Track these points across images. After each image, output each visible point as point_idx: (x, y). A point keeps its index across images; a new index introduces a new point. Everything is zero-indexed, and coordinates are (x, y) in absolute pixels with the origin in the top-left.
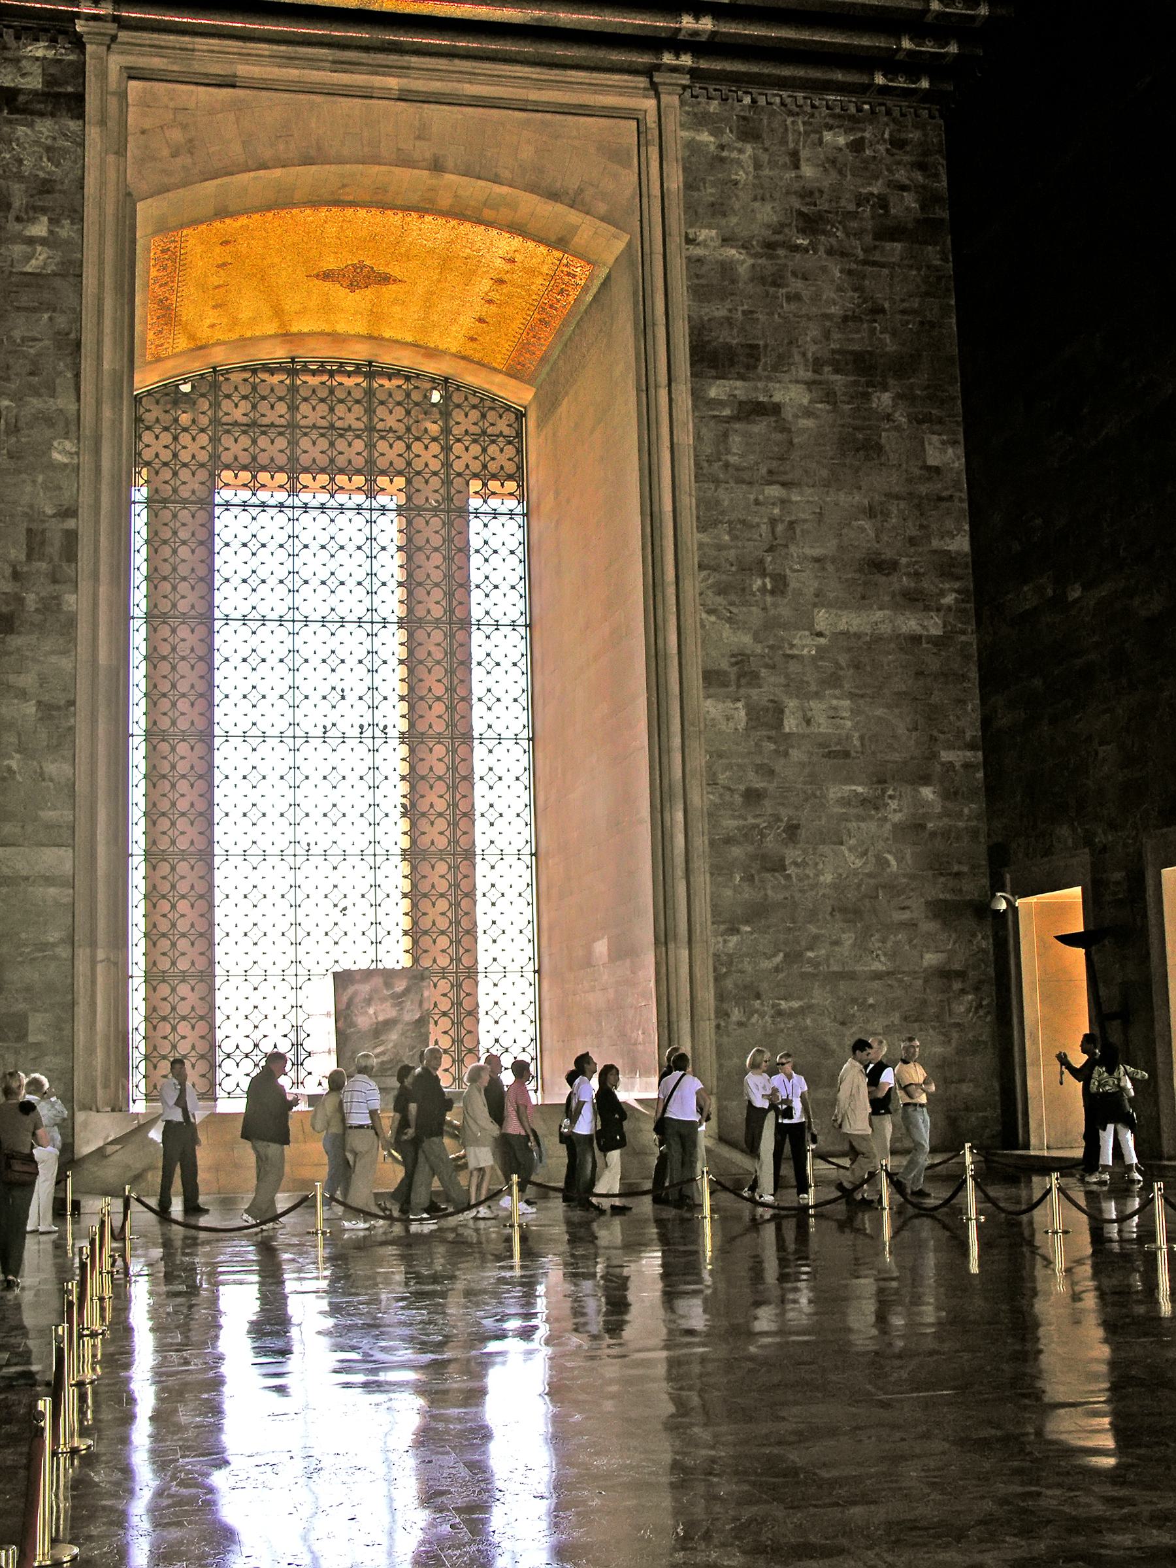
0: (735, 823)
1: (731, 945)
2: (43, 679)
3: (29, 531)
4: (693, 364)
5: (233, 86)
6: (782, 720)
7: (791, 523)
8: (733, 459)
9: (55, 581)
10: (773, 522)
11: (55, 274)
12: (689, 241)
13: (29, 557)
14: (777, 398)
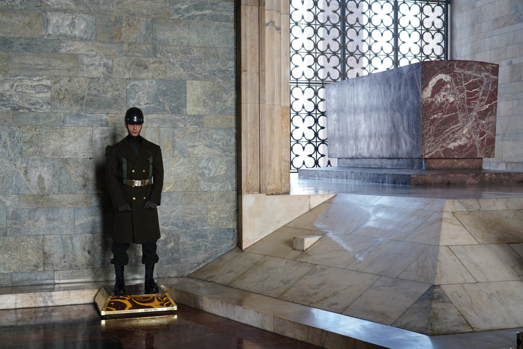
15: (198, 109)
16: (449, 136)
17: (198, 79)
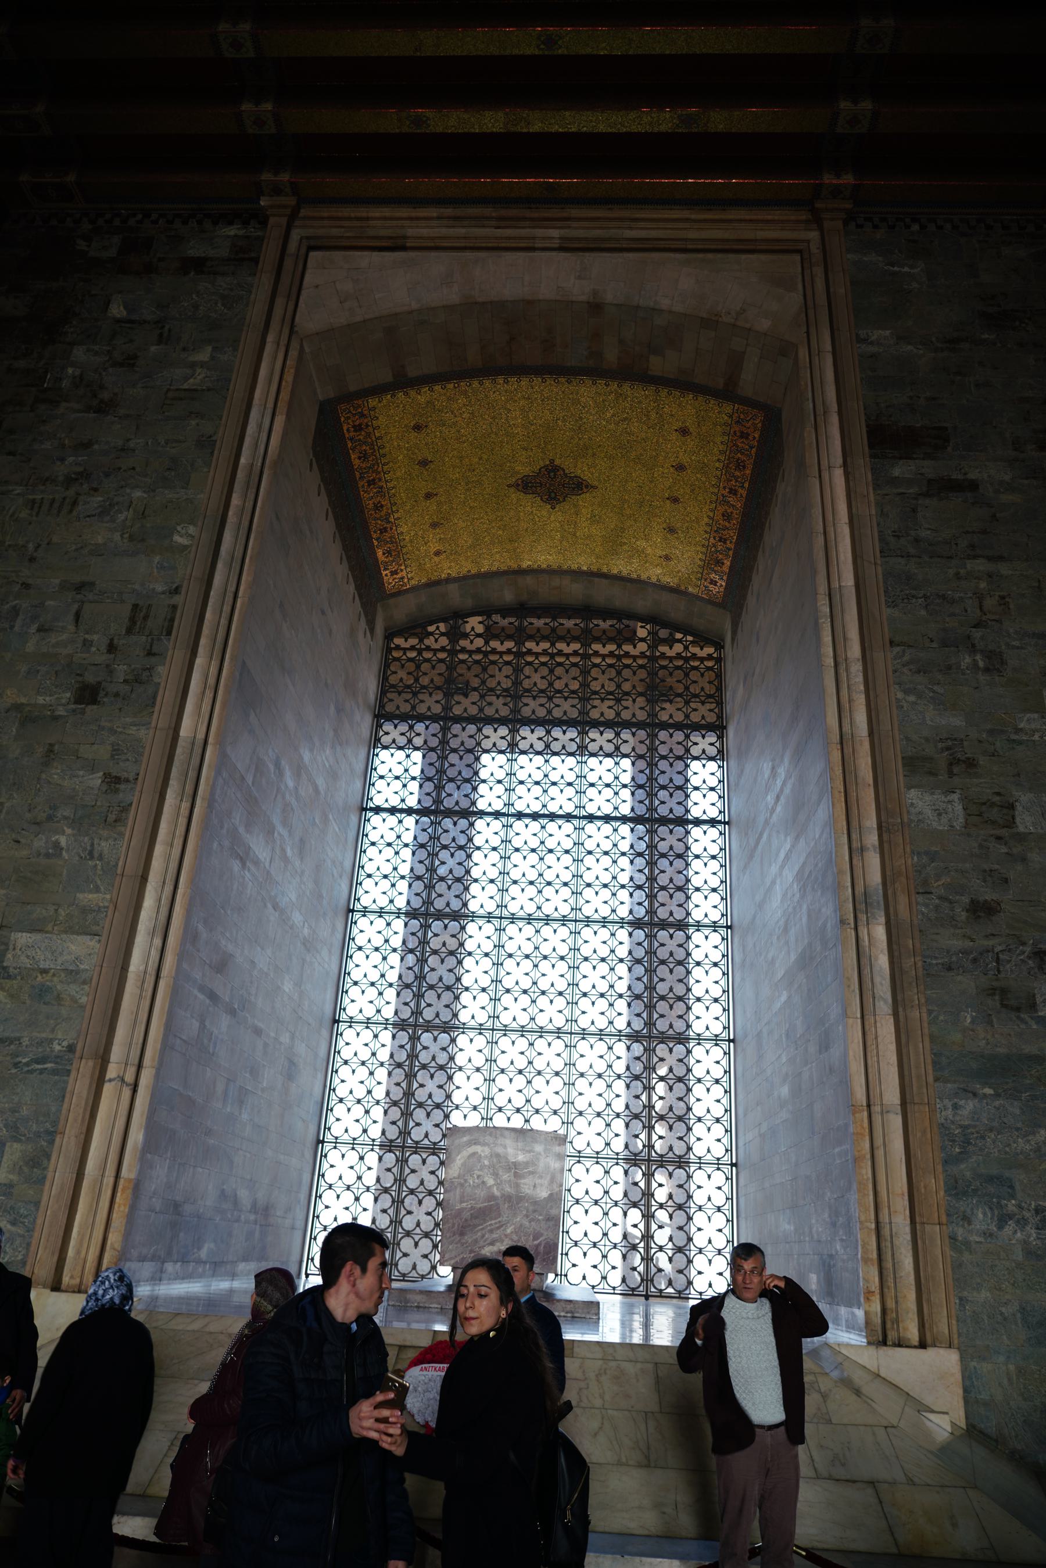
0: (957, 944)
1: (965, 1112)
2: (116, 752)
3: (135, 606)
4: (871, 446)
5: (404, 248)
6: (1013, 817)
7: (1002, 598)
8: (924, 534)
9: (150, 654)
10: (980, 598)
11: (209, 390)
12: (860, 340)
13: (129, 631)
14: (972, 476)
15: (11, 1177)
16: (483, 1236)
17: (19, 1141)
